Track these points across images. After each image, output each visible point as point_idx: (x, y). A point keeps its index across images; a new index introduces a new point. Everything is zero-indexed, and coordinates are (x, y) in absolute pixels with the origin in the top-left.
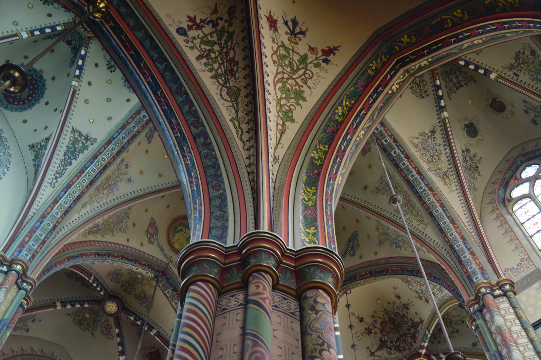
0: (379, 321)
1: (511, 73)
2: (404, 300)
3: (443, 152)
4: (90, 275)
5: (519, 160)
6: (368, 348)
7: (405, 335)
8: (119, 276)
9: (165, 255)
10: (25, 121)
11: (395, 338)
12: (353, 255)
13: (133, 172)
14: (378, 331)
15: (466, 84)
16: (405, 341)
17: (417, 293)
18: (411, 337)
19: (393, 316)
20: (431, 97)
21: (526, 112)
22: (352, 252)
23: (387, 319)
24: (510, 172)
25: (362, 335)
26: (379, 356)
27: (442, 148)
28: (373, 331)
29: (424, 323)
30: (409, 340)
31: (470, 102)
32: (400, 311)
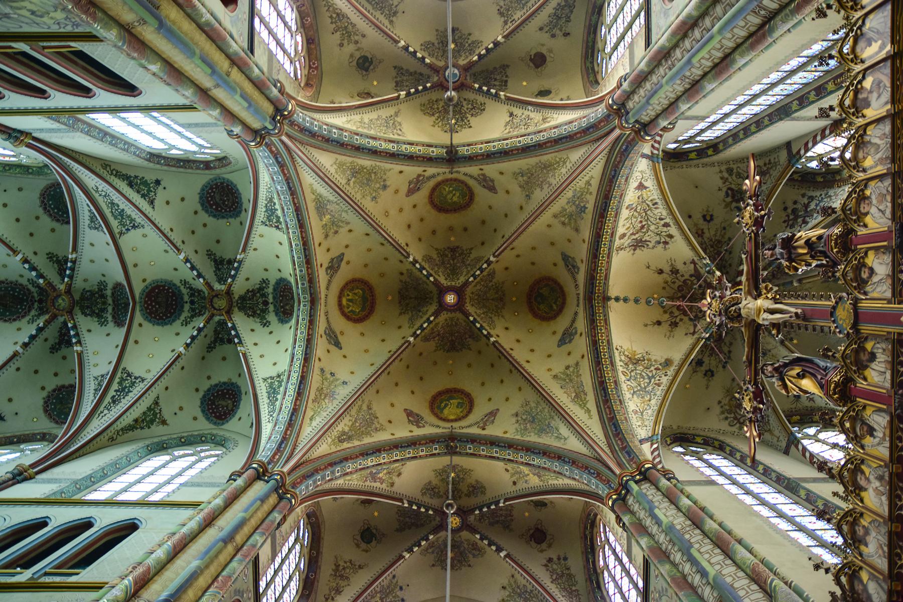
1: (509, 24)
2: (667, 268)
3: (529, 113)
4: (401, 500)
5: (588, 64)
8: (437, 490)
10: (240, 419)
12: (578, 269)
13: (342, 375)
14: (682, 317)
15: (507, 76)
17: (659, 243)
20: (487, 101)
21: (553, 36)
24: (592, 76)
25: (671, 331)
27: (526, 113)
28: (678, 320)
29: (696, 259)
31: (525, 83)
32: (678, 283)
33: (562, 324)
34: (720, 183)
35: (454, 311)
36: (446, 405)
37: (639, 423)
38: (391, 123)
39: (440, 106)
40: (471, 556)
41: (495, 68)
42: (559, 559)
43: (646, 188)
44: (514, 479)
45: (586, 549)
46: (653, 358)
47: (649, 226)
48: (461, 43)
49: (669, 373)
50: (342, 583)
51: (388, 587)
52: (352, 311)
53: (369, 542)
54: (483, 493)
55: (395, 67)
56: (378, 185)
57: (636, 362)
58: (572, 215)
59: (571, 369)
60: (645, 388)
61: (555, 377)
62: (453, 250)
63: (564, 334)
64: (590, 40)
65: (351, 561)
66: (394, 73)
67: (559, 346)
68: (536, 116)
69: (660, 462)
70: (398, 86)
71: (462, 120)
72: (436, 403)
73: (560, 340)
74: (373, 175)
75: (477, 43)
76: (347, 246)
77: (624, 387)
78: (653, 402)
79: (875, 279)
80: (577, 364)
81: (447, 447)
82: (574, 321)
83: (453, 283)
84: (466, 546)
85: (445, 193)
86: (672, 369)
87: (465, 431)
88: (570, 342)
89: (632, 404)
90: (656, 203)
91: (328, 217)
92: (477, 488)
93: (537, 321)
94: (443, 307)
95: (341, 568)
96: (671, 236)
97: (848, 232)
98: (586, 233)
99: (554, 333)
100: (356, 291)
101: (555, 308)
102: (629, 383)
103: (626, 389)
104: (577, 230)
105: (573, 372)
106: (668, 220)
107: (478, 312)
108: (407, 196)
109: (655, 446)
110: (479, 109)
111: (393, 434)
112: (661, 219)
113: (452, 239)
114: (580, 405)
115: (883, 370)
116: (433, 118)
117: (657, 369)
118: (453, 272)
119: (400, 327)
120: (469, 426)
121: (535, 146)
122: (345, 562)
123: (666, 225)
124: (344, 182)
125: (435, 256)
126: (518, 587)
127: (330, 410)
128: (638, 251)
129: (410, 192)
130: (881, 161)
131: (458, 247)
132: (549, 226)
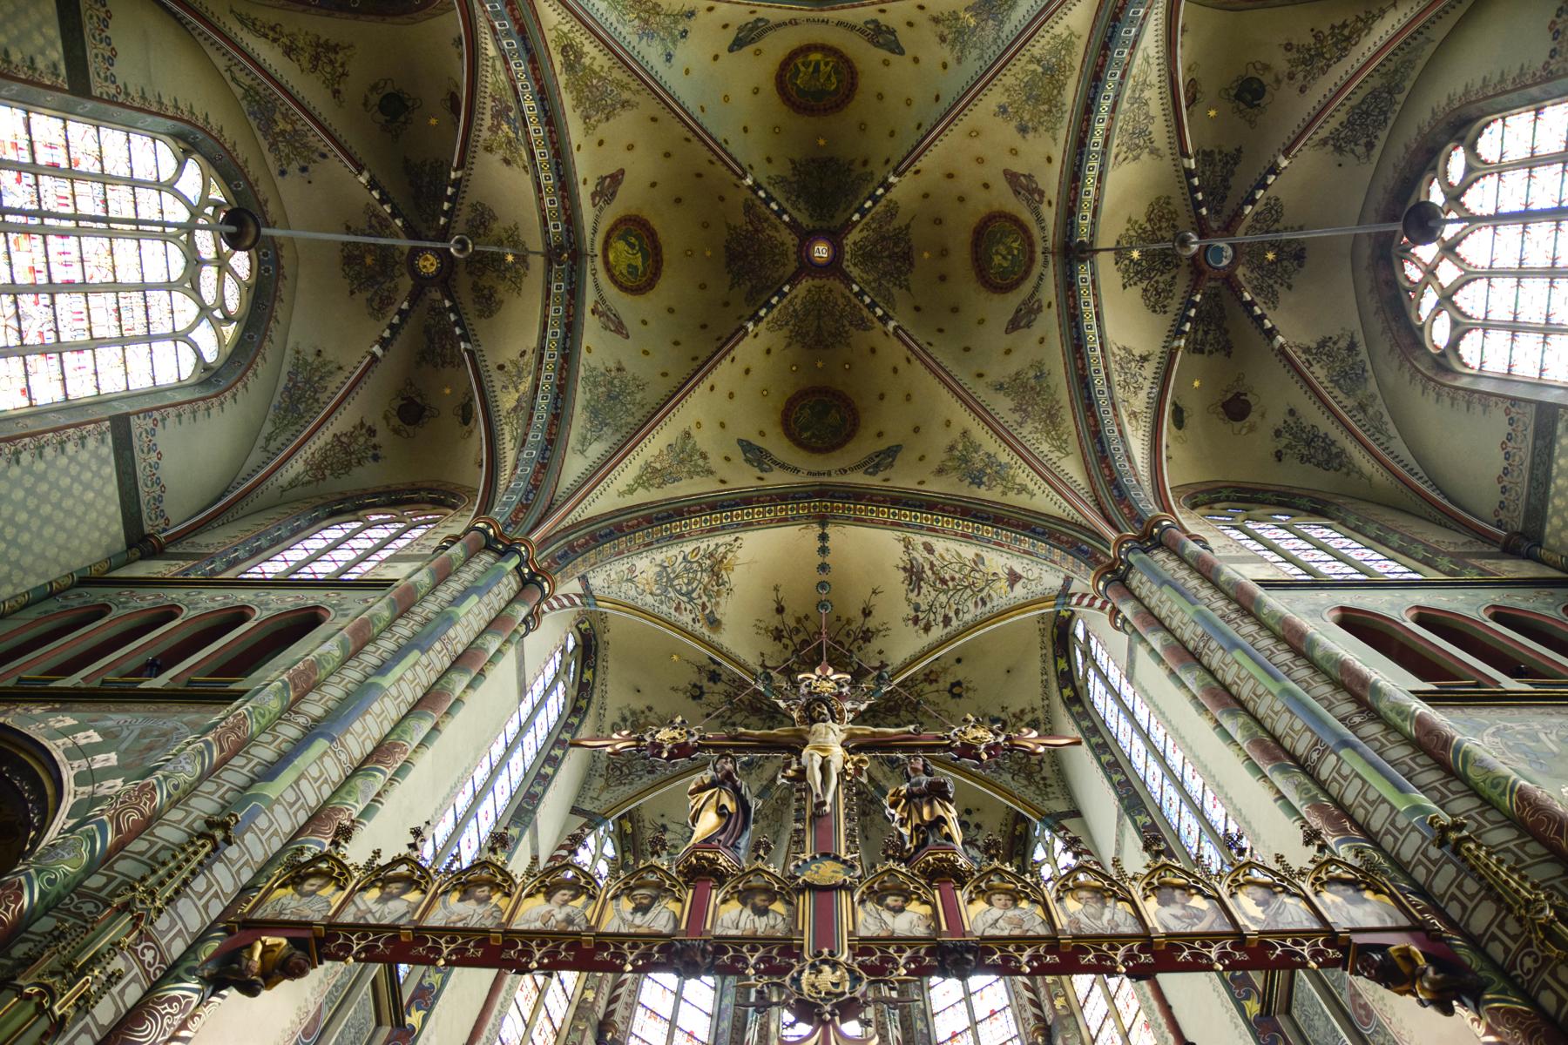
0: (802, 636)
1: (1304, 357)
2: (872, 623)
3: (1146, 389)
5: (1225, 493)
8: (481, 231)
9: (593, 241)
14: (791, 648)
15: (1211, 352)
17: (917, 608)
20: (1170, 316)
21: (1278, 433)
25: (766, 630)
27: (1147, 385)
28: (785, 641)
31: (1196, 384)
33: (777, 445)
34: (1015, 709)
35: (800, 258)
36: (632, 246)
37: (613, 576)
38: (1140, 139)
39: (1163, 233)
40: (369, 295)
41: (1227, 332)
42: (375, 447)
43: (1012, 586)
44: (509, 367)
45: (395, 492)
46: (722, 601)
47: (946, 592)
48: (1274, 272)
49: (697, 626)
50: (305, 59)
51: (305, 146)
52: (798, 71)
53: (382, 108)
54: (481, 315)
55: (1239, 150)
56: (1027, 117)
57: (715, 573)
58: (967, 462)
59: (701, 462)
60: (672, 586)
61: (687, 435)
62: (907, 257)
63: (760, 449)
64: (1268, 496)
65: (344, 74)
66: (1229, 148)
67: (740, 441)
68: (1140, 402)
69: (552, 608)
70: (1205, 156)
71: (1137, 273)
72: (634, 228)
73: (749, 444)
74: (1046, 107)
75: (1273, 300)
76: (916, 60)
77: (674, 551)
78: (650, 599)
79: (886, 915)
80: (710, 472)
81: (561, 247)
82: (783, 466)
83: (848, 256)
84: (385, 286)
85: (1009, 240)
86: (705, 631)
87: (589, 279)
88: (747, 460)
89: (646, 565)
90: (984, 603)
91: (973, 22)
92: (488, 304)
93: (781, 406)
94: (807, 238)
95: (332, 56)
96: (927, 629)
97: (960, 878)
98: (936, 486)
99: (762, 434)
100: (834, 79)
101: (805, 435)
102: (680, 559)
103: (670, 554)
104: (941, 471)
105: (696, 465)
106: (955, 623)
107: (798, 301)
108: (1006, 172)
109: (577, 601)
110: (1157, 302)
111: (579, 148)
112: (957, 612)
113: (926, 255)
114: (640, 477)
115: (741, 924)
116: (1142, 220)
117: (704, 606)
118: (867, 256)
119: (769, 160)
120: (597, 286)
121: (1089, 398)
122: (342, 65)
123: (947, 621)
124: (1036, 51)
125: (896, 223)
126: (321, 378)
127: (620, 28)
128: (902, 575)
129: (1011, 177)
130: (1074, 921)
131: (911, 264)
132: (948, 423)
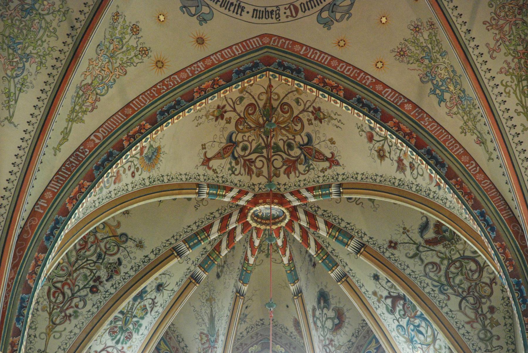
0: (246, 102)
6: (204, 147)
7: (277, 149)
11: (254, 145)
16: (268, 159)
18: (285, 162)
19: (275, 104)
22: (325, 14)
23: (261, 104)
25: (207, 116)
26: (215, 171)
28: (226, 115)
29: (339, 170)
30: (278, 163)
59: (133, 42)
80: (144, 52)
